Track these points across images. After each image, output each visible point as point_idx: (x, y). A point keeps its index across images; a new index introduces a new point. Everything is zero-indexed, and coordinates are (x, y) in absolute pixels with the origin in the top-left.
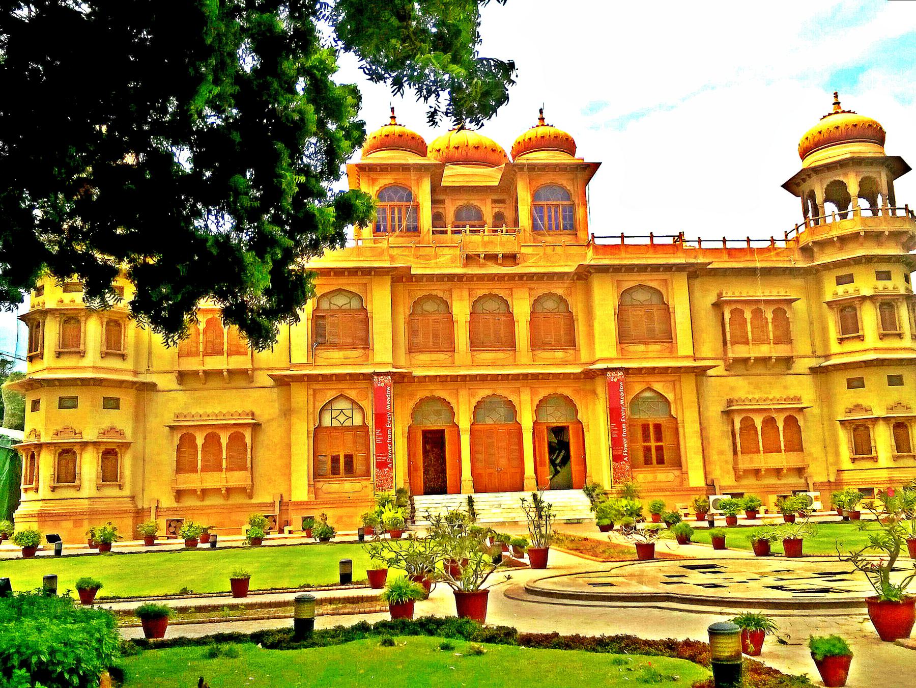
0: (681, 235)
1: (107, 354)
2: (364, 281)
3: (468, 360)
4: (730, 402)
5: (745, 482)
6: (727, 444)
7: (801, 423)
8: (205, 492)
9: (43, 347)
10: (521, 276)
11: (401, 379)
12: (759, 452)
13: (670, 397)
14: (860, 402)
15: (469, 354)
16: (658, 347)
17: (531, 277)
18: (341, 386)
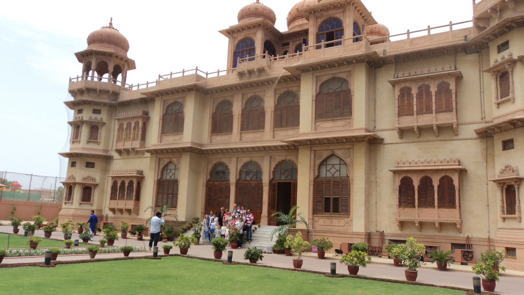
2: (184, 96)
5: (407, 231)
12: (414, 207)
13: (347, 160)
14: (510, 164)
15: (239, 135)
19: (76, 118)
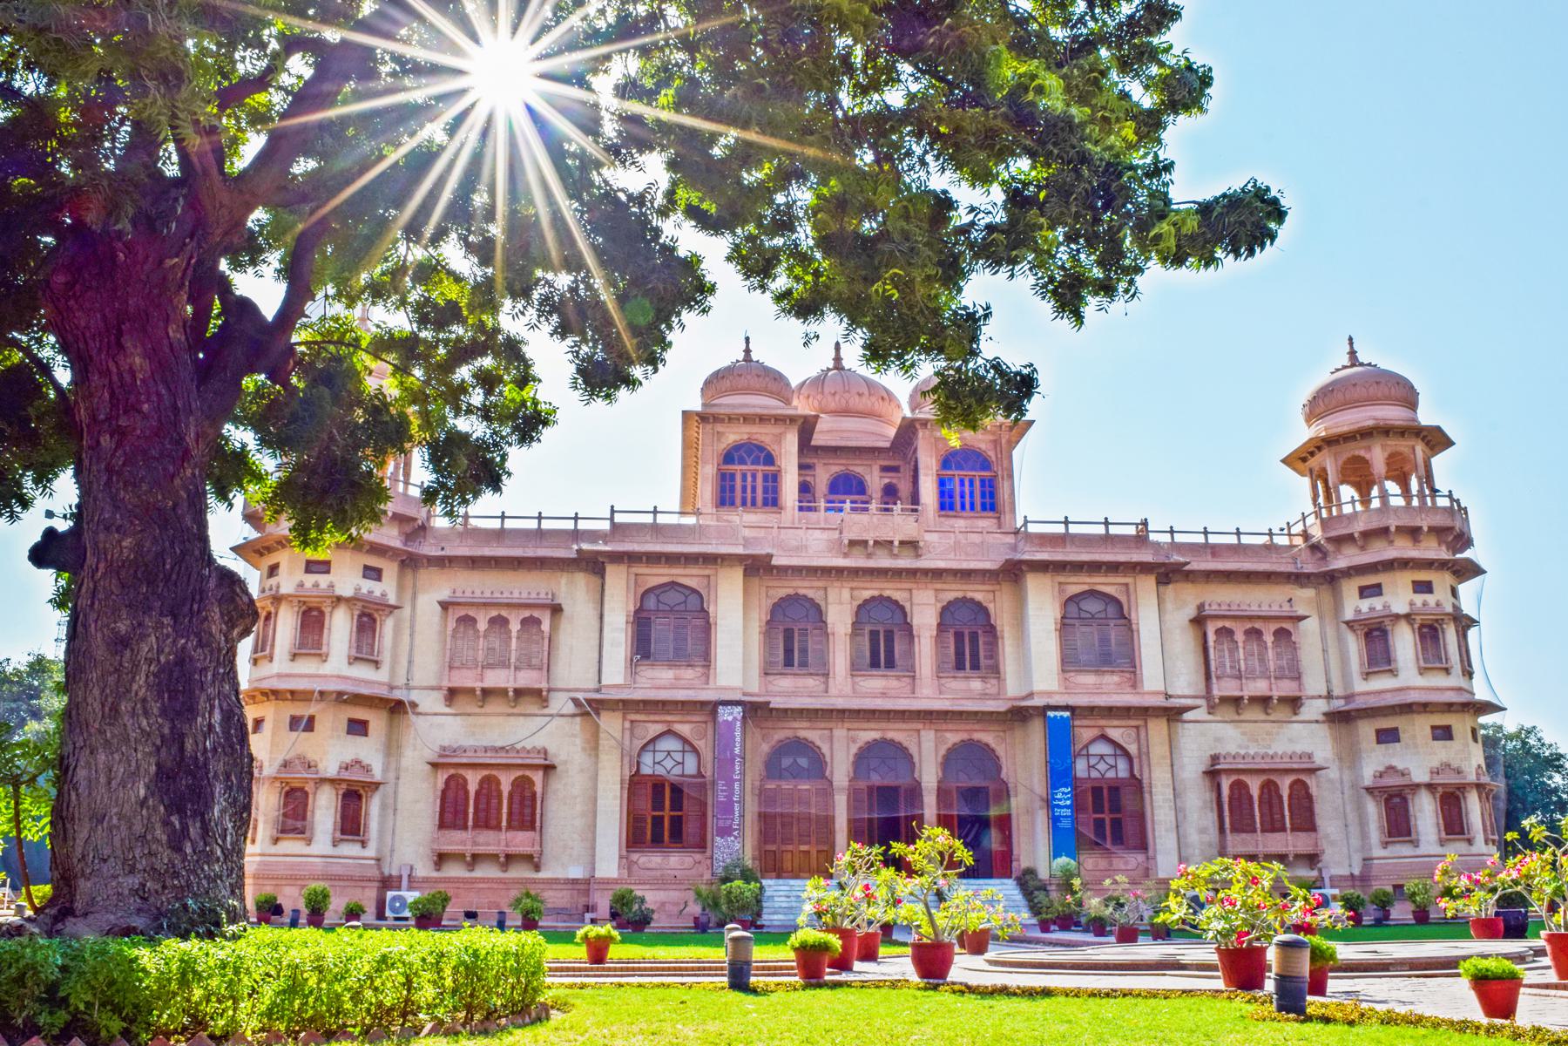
0: (1145, 523)
1: (356, 659)
2: (707, 572)
3: (848, 689)
4: (1215, 759)
6: (1211, 819)
7: (1314, 791)
8: (476, 858)
9: (273, 646)
10: (926, 572)
11: (756, 711)
12: (1254, 831)
13: (1132, 749)
16: (1116, 678)
17: (938, 574)
18: (669, 718)
19: (301, 585)
